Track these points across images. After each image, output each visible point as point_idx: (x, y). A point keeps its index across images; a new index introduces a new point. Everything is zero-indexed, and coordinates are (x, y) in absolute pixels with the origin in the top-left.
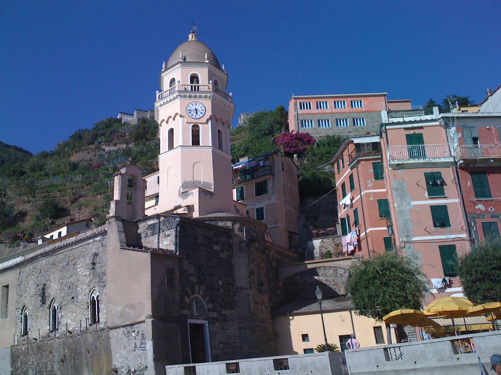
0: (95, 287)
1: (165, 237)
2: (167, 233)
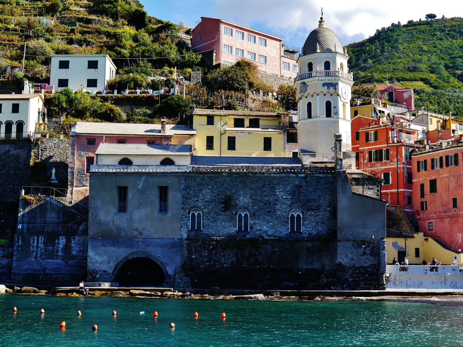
1: (369, 189)
2: (371, 187)
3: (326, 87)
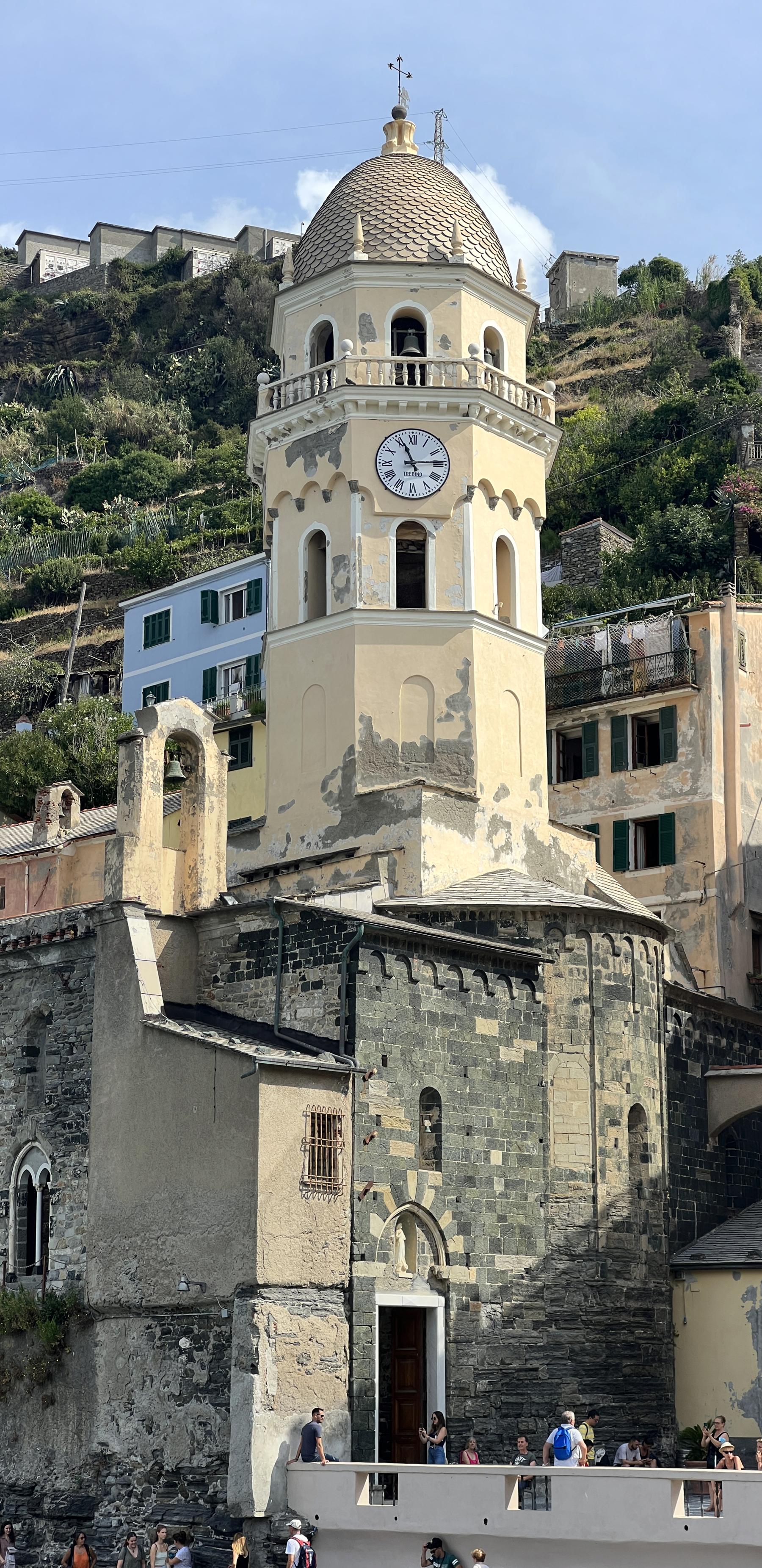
0: (35, 1140)
1: (305, 988)
2: (313, 974)
3: (300, 461)
